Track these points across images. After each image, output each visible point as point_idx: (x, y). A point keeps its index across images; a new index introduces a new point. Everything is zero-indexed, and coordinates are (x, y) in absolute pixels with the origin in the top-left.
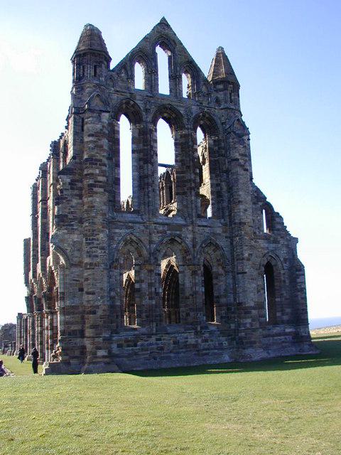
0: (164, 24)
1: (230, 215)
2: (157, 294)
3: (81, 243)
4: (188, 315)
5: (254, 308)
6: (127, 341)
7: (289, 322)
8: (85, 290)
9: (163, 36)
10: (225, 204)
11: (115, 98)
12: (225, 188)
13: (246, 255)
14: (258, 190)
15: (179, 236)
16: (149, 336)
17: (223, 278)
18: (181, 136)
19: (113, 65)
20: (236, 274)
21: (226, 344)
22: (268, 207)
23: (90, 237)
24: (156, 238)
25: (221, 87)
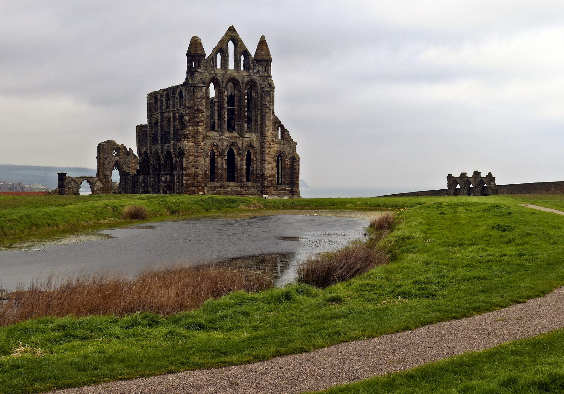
0: (232, 29)
2: (225, 168)
4: (238, 178)
5: (269, 177)
6: (211, 188)
7: (288, 184)
8: (195, 166)
9: (232, 34)
10: (259, 126)
11: (208, 77)
12: (259, 118)
13: (267, 152)
14: (277, 118)
15: (235, 143)
16: (221, 187)
17: (255, 162)
19: (206, 58)
20: (263, 160)
22: (282, 127)
23: (196, 144)
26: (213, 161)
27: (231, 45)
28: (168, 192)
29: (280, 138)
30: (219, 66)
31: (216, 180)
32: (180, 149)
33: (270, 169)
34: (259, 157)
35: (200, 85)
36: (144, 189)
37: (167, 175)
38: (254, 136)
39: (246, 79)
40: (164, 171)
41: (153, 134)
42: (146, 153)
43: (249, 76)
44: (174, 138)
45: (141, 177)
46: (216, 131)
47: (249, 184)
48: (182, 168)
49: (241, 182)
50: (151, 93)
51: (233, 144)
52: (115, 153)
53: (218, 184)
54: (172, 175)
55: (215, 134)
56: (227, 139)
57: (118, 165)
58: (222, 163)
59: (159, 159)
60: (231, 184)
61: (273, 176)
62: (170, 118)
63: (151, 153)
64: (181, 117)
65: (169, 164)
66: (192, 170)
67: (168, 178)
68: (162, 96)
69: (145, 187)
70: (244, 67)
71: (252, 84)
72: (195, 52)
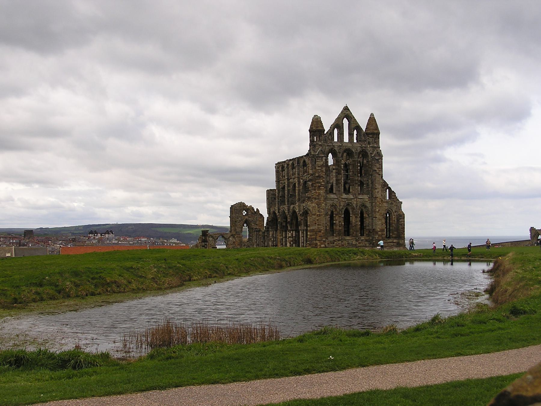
0: (346, 109)
1: (372, 194)
3: (315, 207)
6: (331, 242)
7: (395, 238)
9: (346, 113)
12: (370, 182)
15: (351, 203)
16: (339, 241)
17: (367, 219)
18: (353, 161)
20: (373, 217)
21: (368, 245)
22: (389, 189)
23: (319, 204)
24: (342, 204)
25: (371, 136)
26: (332, 218)
27: (345, 122)
28: (294, 245)
29: (388, 199)
30: (336, 139)
31: (335, 235)
32: (304, 209)
33: (379, 225)
34: (370, 215)
35: (321, 155)
36: (273, 243)
37: (293, 231)
38: (366, 197)
39: (359, 149)
40: (291, 228)
41: (281, 197)
42: (274, 213)
43: (361, 147)
44: (299, 200)
45: (271, 233)
46: (335, 194)
47: (363, 238)
48: (307, 226)
49: (357, 236)
50: (279, 163)
51: (348, 205)
52: (245, 213)
53: (337, 238)
54: (297, 231)
55: (332, 196)
56: (344, 200)
57: (246, 222)
58: (339, 220)
59: (286, 218)
60: (348, 238)
61: (382, 230)
62: (295, 184)
63: (279, 212)
64: (305, 183)
65: (294, 222)
66: (315, 227)
67: (294, 234)
68: (288, 165)
69: (273, 241)
70: (357, 139)
71: (364, 154)
72: (316, 128)
